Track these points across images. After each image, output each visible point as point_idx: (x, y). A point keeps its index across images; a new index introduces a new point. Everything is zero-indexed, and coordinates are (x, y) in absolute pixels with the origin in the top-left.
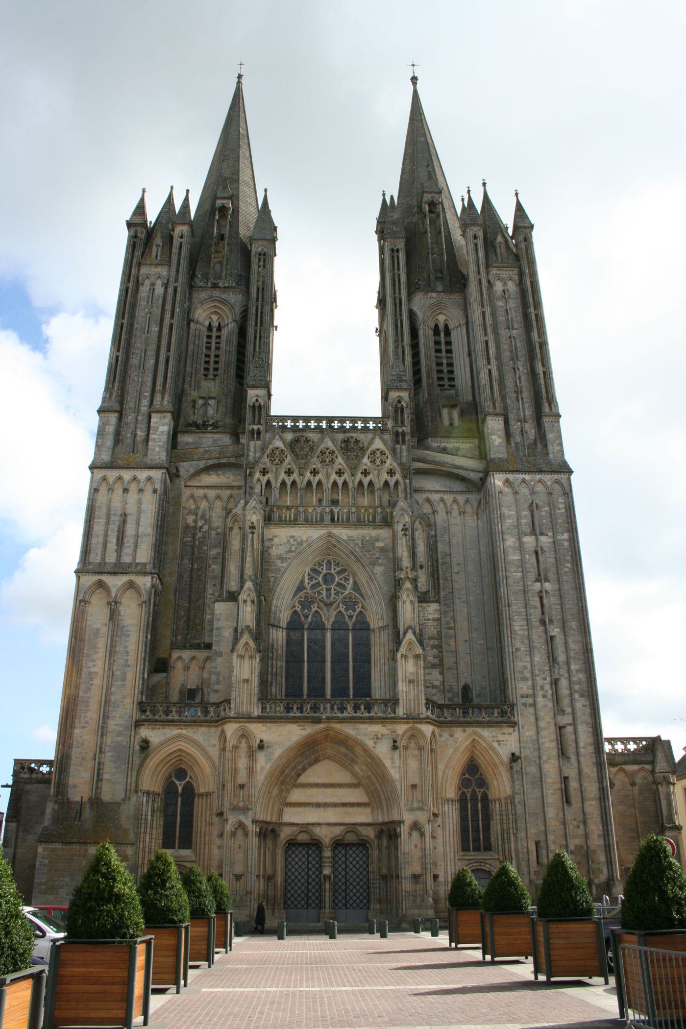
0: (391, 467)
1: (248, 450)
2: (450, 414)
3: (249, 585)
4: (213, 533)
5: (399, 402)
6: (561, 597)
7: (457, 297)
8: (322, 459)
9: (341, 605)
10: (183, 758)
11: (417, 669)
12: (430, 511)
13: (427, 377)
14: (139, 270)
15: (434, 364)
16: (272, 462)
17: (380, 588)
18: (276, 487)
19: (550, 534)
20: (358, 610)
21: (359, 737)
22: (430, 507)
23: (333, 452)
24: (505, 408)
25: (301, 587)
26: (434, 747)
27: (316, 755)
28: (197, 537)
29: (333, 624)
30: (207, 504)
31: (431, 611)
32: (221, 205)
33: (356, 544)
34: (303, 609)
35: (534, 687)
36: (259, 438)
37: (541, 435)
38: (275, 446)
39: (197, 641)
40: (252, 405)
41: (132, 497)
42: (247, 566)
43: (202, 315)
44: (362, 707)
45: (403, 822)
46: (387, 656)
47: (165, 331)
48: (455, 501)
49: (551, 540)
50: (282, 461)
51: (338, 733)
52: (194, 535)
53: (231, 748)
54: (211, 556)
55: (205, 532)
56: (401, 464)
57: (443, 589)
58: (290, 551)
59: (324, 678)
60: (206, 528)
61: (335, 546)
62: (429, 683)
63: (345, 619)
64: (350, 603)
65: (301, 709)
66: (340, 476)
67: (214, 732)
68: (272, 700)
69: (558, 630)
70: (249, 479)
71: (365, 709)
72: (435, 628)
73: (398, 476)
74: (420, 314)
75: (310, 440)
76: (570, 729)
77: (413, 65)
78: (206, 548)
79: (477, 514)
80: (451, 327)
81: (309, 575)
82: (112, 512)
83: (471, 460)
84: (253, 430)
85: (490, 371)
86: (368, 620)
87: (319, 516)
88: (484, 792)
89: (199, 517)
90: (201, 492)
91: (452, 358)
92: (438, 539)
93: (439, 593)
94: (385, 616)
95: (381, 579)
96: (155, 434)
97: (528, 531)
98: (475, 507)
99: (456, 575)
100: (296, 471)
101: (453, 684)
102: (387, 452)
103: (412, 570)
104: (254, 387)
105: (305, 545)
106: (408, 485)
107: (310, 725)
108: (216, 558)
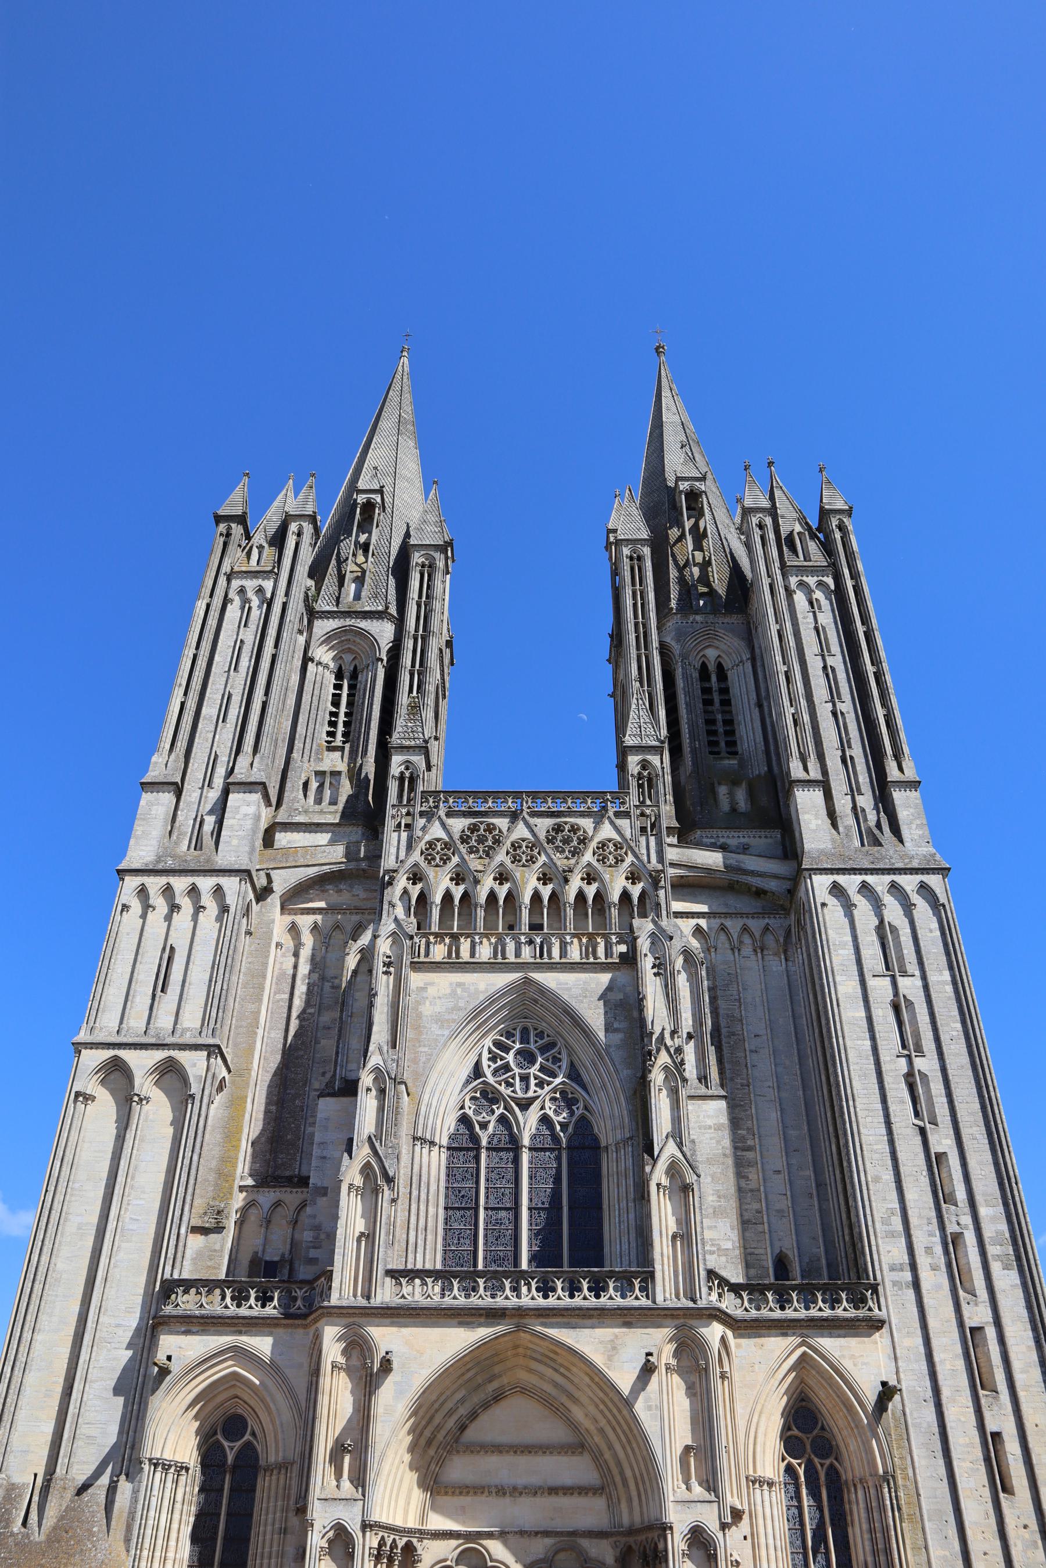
2: (731, 794)
4: (327, 985)
7: (735, 619)
8: (515, 857)
9: (548, 1104)
13: (690, 738)
15: (701, 721)
16: (429, 863)
17: (617, 1071)
24: (825, 772)
25: (477, 1071)
27: (495, 1385)
29: (533, 1137)
31: (711, 1113)
32: (365, 500)
34: (477, 1112)
39: (287, 1173)
44: (585, 1285)
45: (671, 1528)
46: (631, 1196)
53: (329, 1367)
54: (321, 1025)
57: (732, 1079)
58: (456, 1008)
61: (536, 1001)
62: (713, 1245)
67: (300, 1336)
72: (718, 1142)
76: (991, 1333)
79: (785, 952)
80: (727, 664)
81: (490, 1051)
83: (772, 861)
86: (596, 1130)
88: (831, 1465)
91: (730, 712)
92: (719, 993)
94: (626, 1120)
95: (617, 1056)
98: (782, 940)
103: (673, 1033)
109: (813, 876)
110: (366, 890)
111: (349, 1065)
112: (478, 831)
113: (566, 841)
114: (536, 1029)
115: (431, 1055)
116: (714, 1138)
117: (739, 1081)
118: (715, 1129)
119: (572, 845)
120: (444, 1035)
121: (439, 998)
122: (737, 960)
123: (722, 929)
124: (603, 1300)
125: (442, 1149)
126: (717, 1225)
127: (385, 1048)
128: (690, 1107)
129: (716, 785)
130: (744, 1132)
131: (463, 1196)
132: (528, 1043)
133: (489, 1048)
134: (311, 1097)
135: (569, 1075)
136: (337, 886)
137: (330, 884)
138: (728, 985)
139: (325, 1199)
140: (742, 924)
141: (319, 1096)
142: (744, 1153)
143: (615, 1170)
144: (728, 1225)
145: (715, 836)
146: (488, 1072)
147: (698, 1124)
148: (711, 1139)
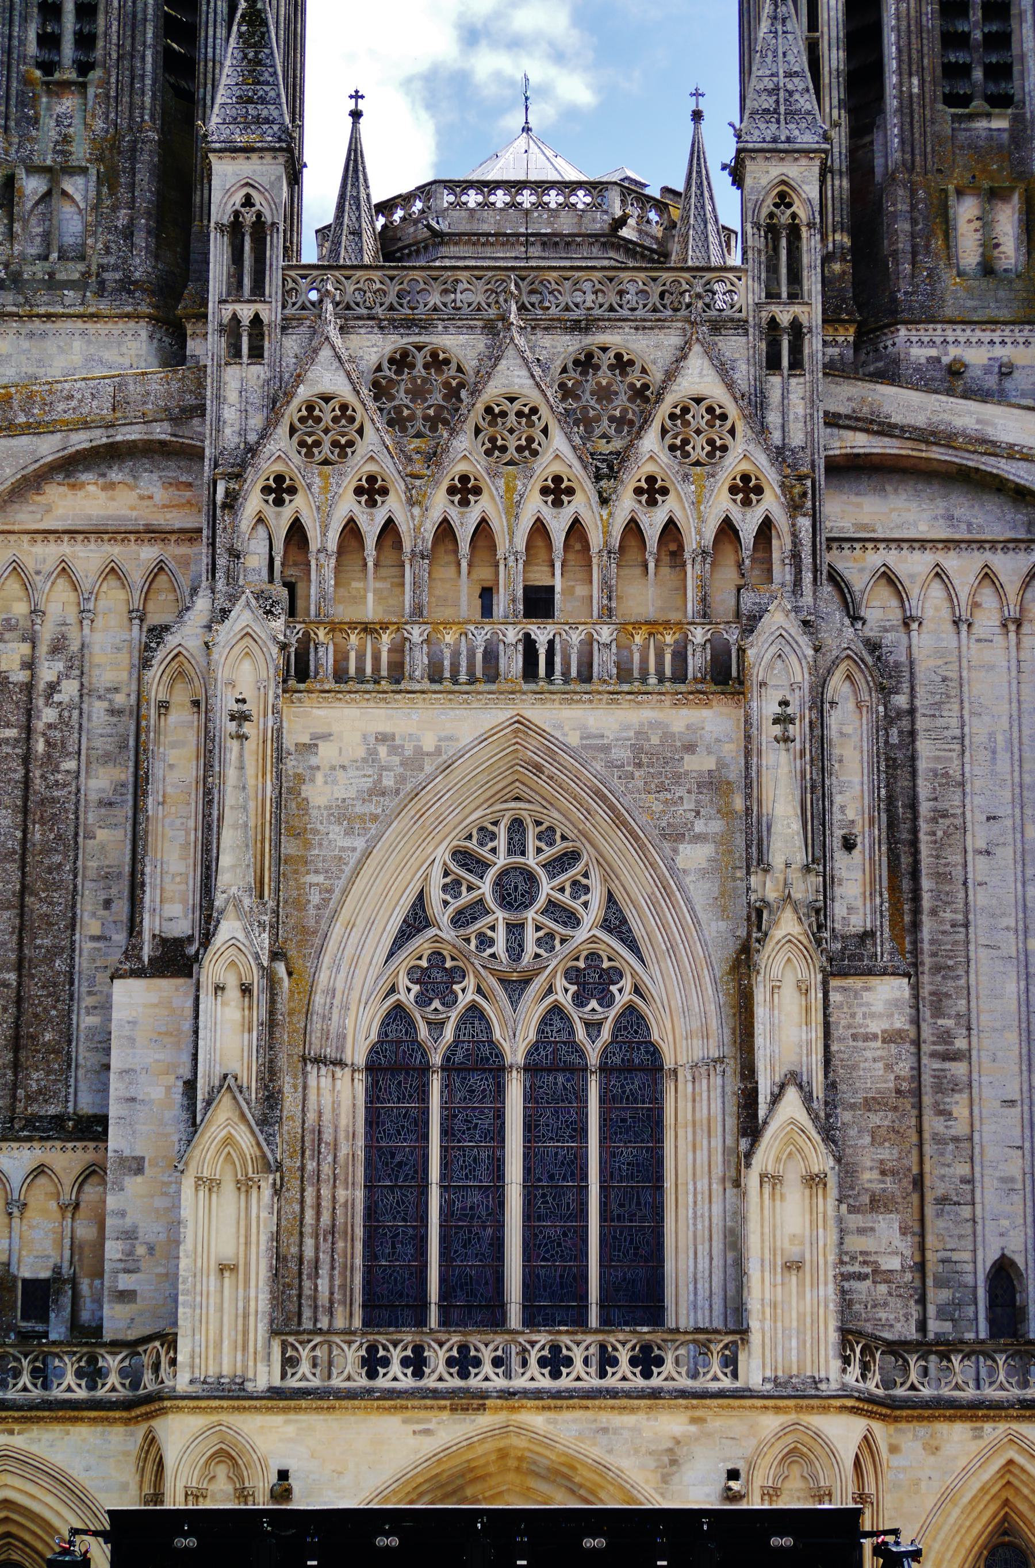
0: (745, 467)
1: (219, 398)
2: (985, 222)
3: (229, 929)
4: (98, 709)
5: (783, 200)
8: (493, 440)
9: (560, 982)
10: (14, 1529)
11: (813, 1224)
12: (895, 616)
16: (309, 454)
18: (323, 550)
20: (621, 1000)
21: (609, 1460)
22: (894, 603)
23: (534, 411)
26: (870, 1489)
28: (39, 725)
29: (534, 1049)
30: (72, 596)
31: (879, 1007)
33: (610, 765)
34: (423, 1001)
36: (257, 353)
38: (320, 389)
39: (52, 1110)
40: (227, 219)
42: (226, 860)
46: (718, 1171)
48: (988, 576)
50: (344, 449)
51: (541, 1444)
52: (29, 713)
54: (93, 797)
55: (70, 707)
56: (780, 454)
57: (934, 912)
58: (378, 791)
59: (498, 1244)
60: (69, 689)
61: (539, 768)
62: (865, 1263)
63: (572, 1032)
65: (417, 1363)
66: (558, 503)
68: (320, 1332)
70: (224, 519)
71: (633, 1362)
72: (889, 1067)
75: (447, 362)
78: (70, 765)
81: (446, 874)
84: (235, 318)
86: (655, 1036)
87: (479, 657)
89: (43, 649)
90: (49, 553)
92: (921, 723)
93: (916, 926)
94: (714, 1024)
99: (981, 859)
100: (398, 488)
101: (955, 1256)
102: (732, 411)
103: (807, 869)
105: (428, 769)
106: (806, 536)
107: (445, 1415)
108: (111, 804)
110: (168, 484)
111: (166, 906)
112: (412, 366)
113: (604, 394)
114: (538, 823)
115: (330, 891)
116: (882, 1058)
117: (948, 915)
118: (884, 1041)
119: (616, 403)
120: (354, 849)
121: (343, 767)
122: (964, 649)
123: (937, 574)
124: (655, 1382)
125: (356, 1075)
126: (876, 1225)
127: (247, 902)
128: (835, 997)
129: (952, 200)
130: (949, 1023)
131: (400, 1164)
132: (523, 853)
133: (445, 864)
134: (85, 953)
135: (605, 920)
136: (104, 475)
137: (87, 469)
138: (939, 704)
139: (139, 1179)
140: (981, 564)
141: (112, 978)
142: (947, 1065)
143: (690, 1117)
144: (896, 1226)
145: (938, 340)
146: (444, 917)
147: (851, 1031)
148: (875, 1060)
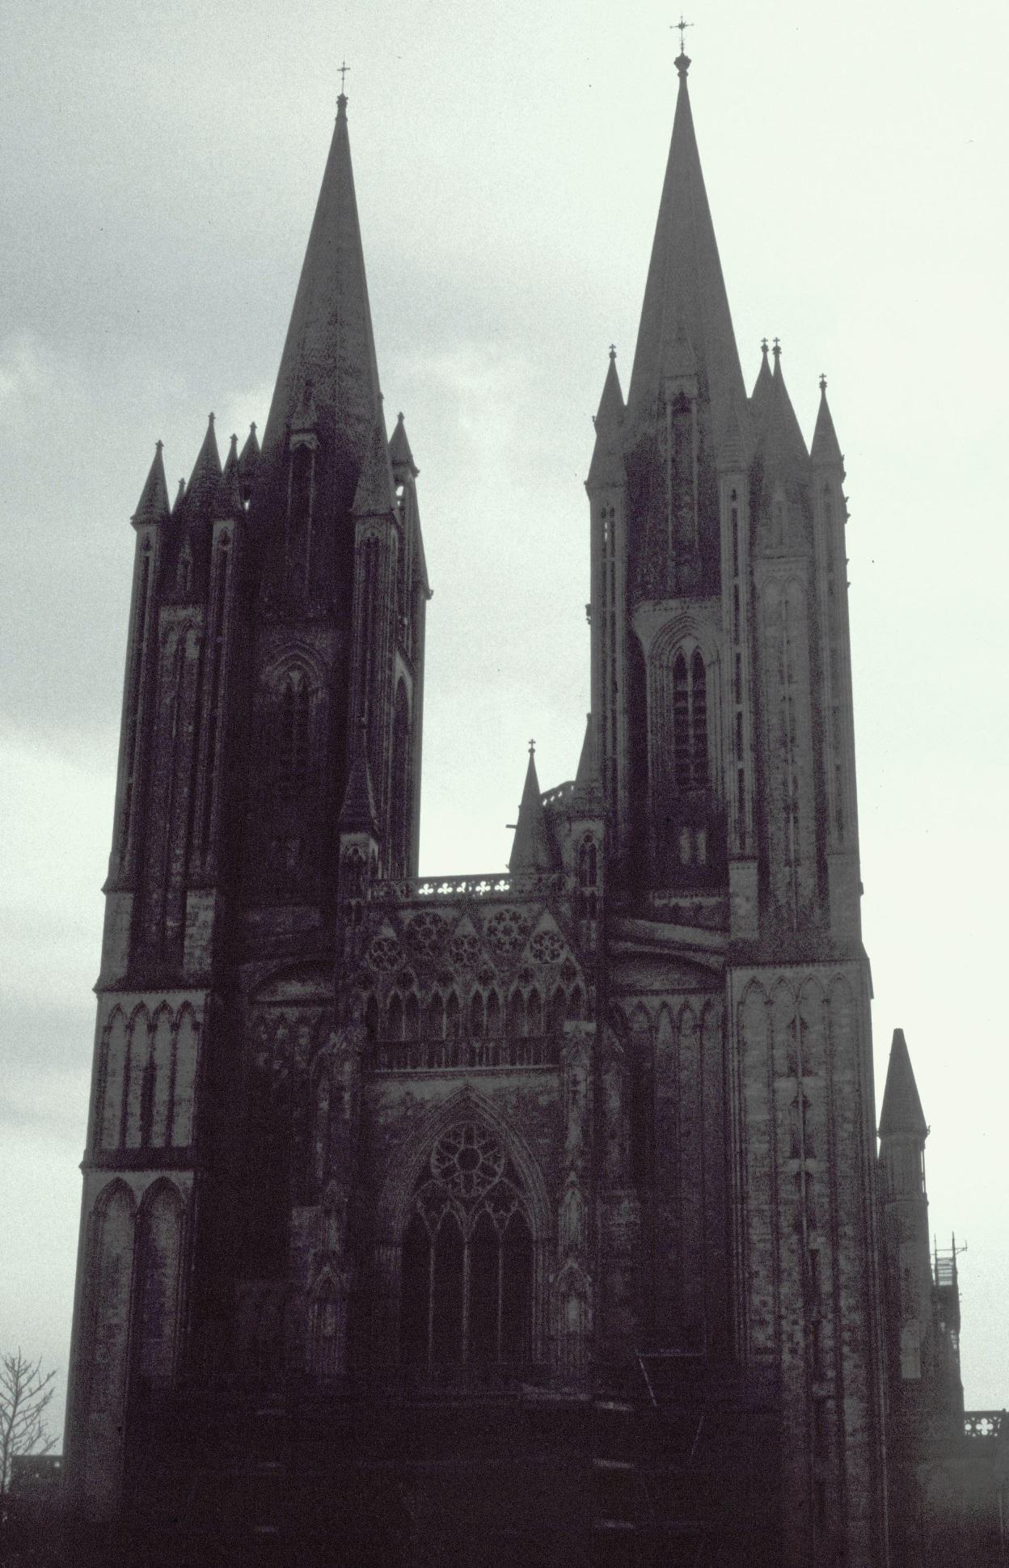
5: (588, 839)
6: (833, 1184)
14: (157, 614)
19: (822, 1073)
20: (513, 1209)
25: (426, 1174)
32: (298, 445)
35: (778, 1334)
37: (822, 890)
41: (164, 1035)
43: (277, 675)
47: (204, 735)
49: (822, 1083)
64: (501, 1199)
69: (823, 1239)
73: (580, 981)
74: (646, 647)
77: (682, 26)
81: (439, 1153)
82: (133, 1063)
85: (741, 772)
96: (194, 925)
97: (785, 1070)
104: (352, 828)
109: (733, 972)
146: (435, 1171)
